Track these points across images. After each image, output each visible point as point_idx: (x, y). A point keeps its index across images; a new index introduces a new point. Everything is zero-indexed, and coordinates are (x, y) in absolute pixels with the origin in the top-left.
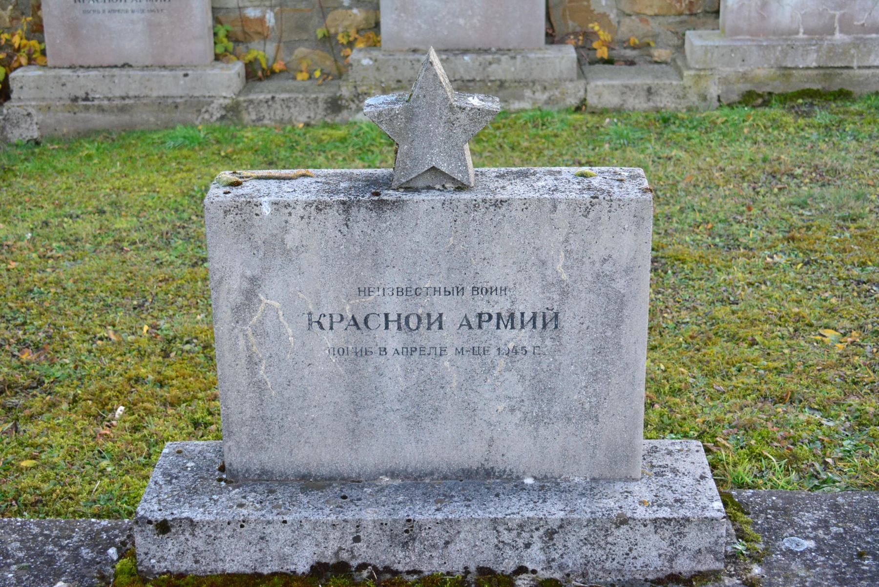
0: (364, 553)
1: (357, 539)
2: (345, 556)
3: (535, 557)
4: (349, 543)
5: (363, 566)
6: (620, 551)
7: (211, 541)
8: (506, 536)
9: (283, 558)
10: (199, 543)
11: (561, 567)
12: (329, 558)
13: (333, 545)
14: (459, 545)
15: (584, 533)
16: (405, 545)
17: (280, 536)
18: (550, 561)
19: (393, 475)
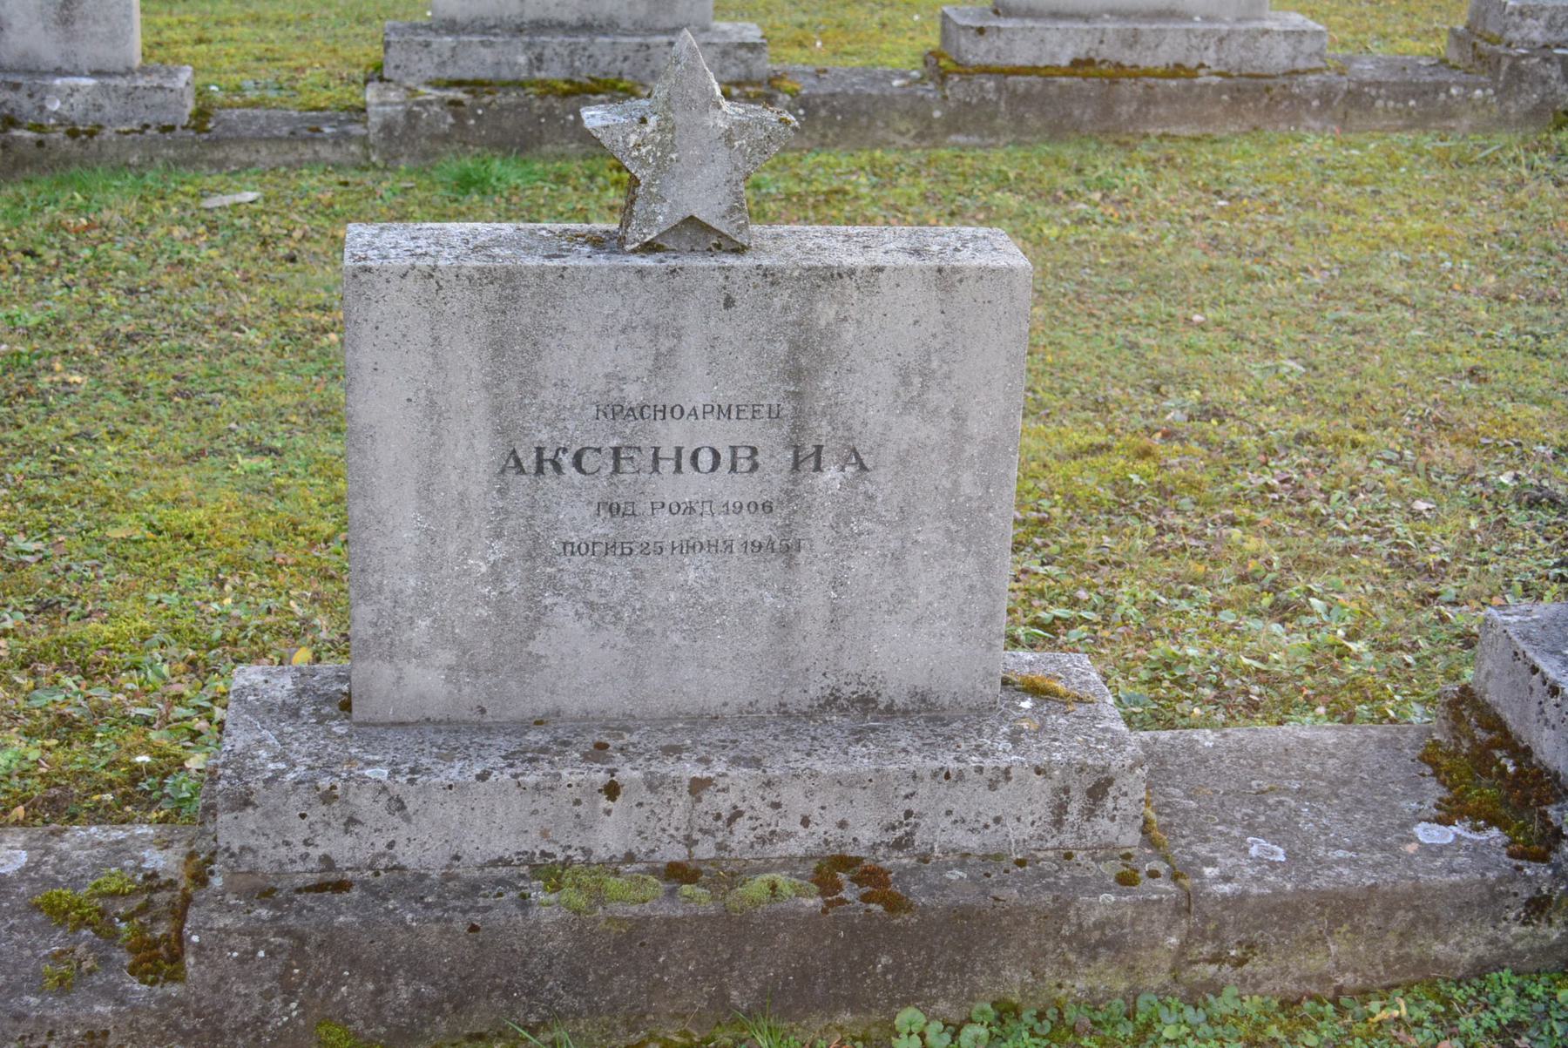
0: (1105, 52)
1: (1101, 42)
2: (1092, 54)
3: (1210, 57)
4: (1096, 45)
5: (1103, 62)
6: (1262, 53)
7: (1010, 41)
8: (1194, 41)
9: (1053, 55)
10: (1000, 44)
11: (1226, 64)
12: (1082, 56)
13: (1086, 46)
14: (1164, 47)
15: (1242, 39)
16: (1131, 47)
17: (1054, 38)
18: (1219, 60)
19: (1112, 12)
